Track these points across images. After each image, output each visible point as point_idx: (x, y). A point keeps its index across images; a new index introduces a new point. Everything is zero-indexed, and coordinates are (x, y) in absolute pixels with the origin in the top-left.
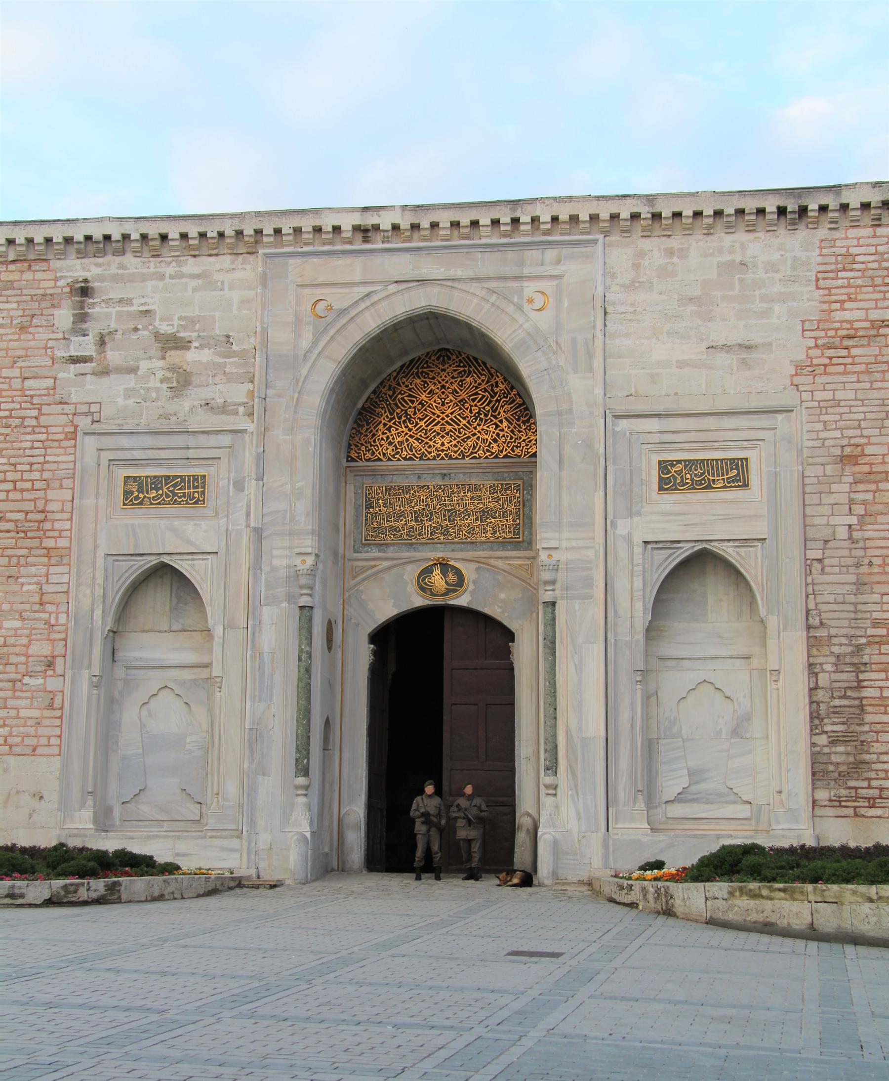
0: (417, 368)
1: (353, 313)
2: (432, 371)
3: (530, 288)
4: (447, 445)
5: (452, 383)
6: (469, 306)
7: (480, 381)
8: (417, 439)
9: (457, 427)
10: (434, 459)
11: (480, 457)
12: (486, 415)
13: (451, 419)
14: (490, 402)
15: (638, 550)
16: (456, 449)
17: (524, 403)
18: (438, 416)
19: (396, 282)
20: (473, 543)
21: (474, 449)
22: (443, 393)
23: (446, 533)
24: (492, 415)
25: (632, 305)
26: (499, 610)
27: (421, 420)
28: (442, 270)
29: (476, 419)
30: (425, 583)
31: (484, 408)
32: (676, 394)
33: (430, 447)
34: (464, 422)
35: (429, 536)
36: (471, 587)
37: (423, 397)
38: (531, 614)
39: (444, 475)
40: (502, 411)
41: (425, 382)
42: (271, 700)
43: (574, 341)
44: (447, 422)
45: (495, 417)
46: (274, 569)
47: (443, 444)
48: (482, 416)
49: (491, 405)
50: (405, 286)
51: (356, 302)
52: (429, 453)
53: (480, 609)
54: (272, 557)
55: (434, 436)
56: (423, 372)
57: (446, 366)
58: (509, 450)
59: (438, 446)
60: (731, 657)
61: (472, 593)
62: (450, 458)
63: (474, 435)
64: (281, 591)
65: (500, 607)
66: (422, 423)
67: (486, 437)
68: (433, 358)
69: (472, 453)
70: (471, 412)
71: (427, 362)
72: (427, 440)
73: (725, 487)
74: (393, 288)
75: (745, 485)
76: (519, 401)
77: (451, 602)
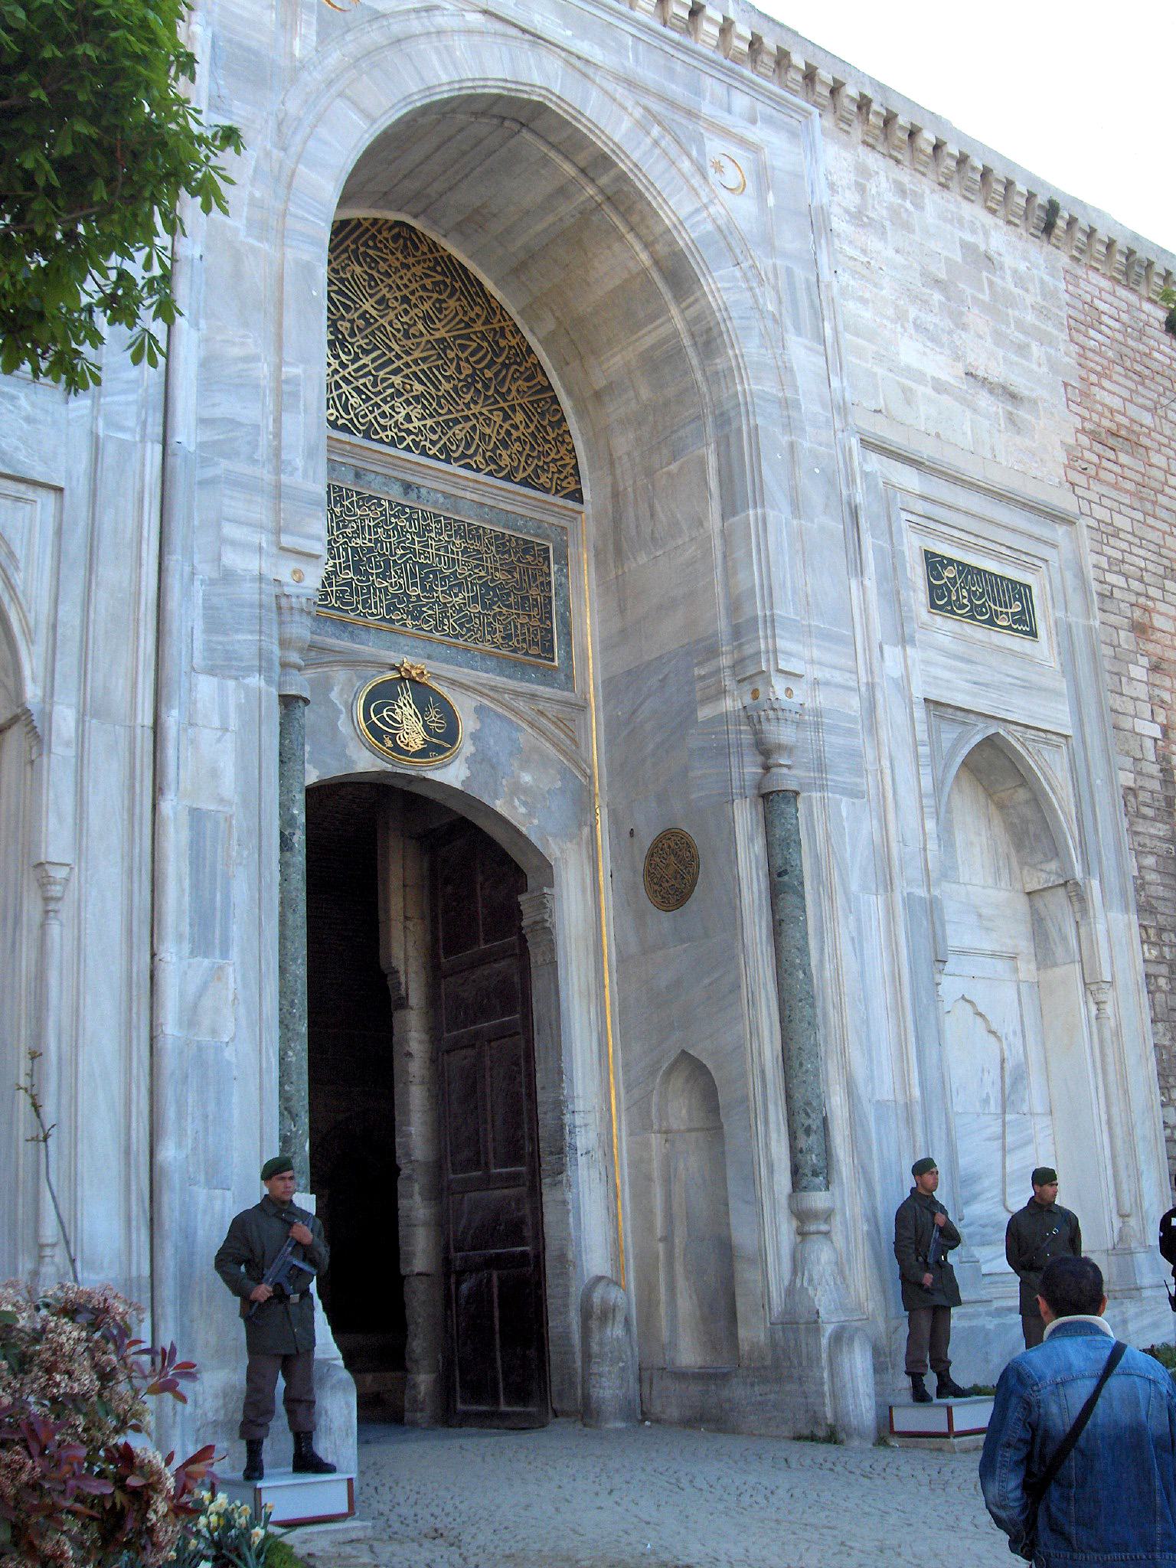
0: (355, 242)
1: (397, 28)
2: (385, 260)
3: (715, 146)
4: (417, 423)
5: (421, 297)
6: (613, 122)
7: (472, 315)
8: (357, 389)
9: (433, 391)
10: (392, 444)
11: (478, 470)
12: (487, 387)
13: (423, 371)
14: (492, 363)
15: (920, 713)
16: (435, 437)
17: (550, 388)
18: (399, 357)
19: (485, 12)
20: (467, 650)
21: (468, 446)
22: (406, 312)
23: (416, 614)
24: (497, 391)
25: (864, 252)
26: (523, 810)
27: (367, 352)
28: (569, 33)
29: (468, 386)
30: (382, 720)
31: (481, 370)
32: (938, 435)
33: (383, 415)
34: (447, 386)
35: (384, 611)
36: (466, 746)
37: (367, 306)
38: (580, 827)
39: (407, 487)
40: (514, 388)
41: (372, 277)
42: (225, 953)
43: (789, 272)
44: (415, 374)
45: (506, 401)
46: (228, 577)
47: (408, 418)
48: (479, 386)
49: (495, 368)
50: (499, 26)
51: (408, 11)
52: (384, 428)
53: (486, 800)
54: (223, 541)
55: (392, 396)
56: (366, 254)
57: (411, 260)
58: (530, 470)
59: (400, 418)
60: (993, 955)
61: (471, 761)
62: (424, 453)
63: (467, 418)
64: (245, 641)
65: (525, 804)
66: (366, 360)
67: (488, 431)
68: (385, 234)
69: (464, 456)
70: (459, 370)
71: (373, 237)
72: (378, 400)
73: (1009, 628)
74: (475, 19)
75: (1033, 634)
76: (540, 377)
77: (430, 775)
